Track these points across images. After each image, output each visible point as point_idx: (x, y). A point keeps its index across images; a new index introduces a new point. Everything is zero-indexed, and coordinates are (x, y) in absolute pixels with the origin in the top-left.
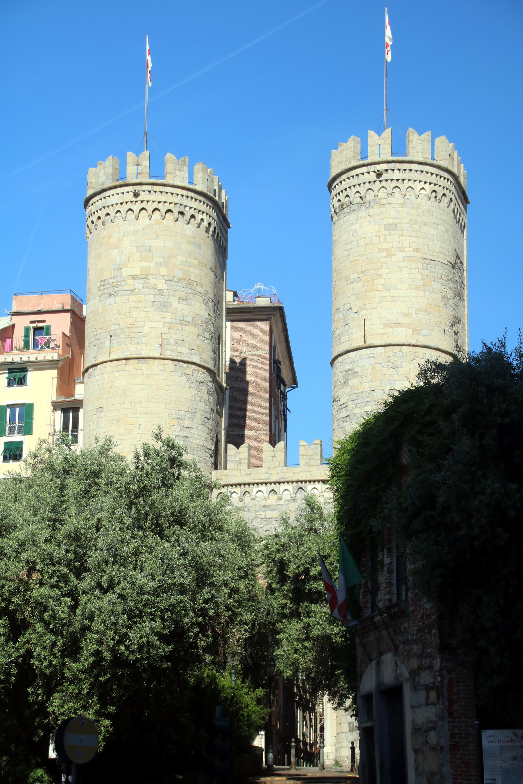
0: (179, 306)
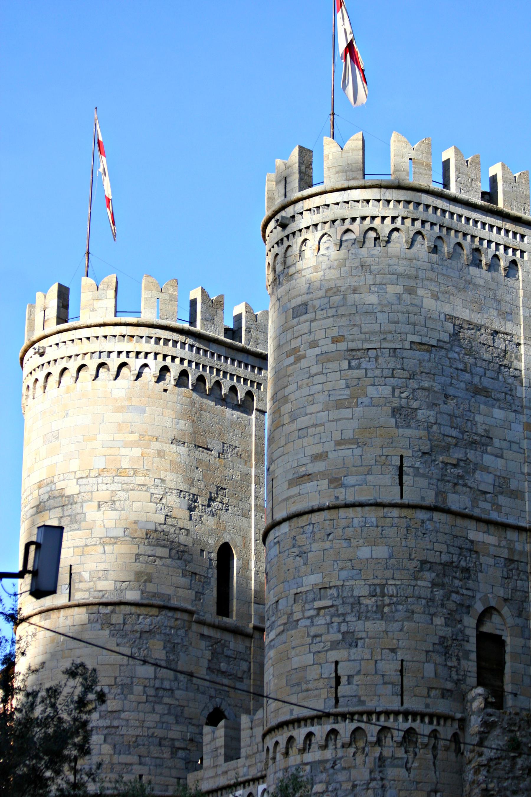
0: (99, 515)
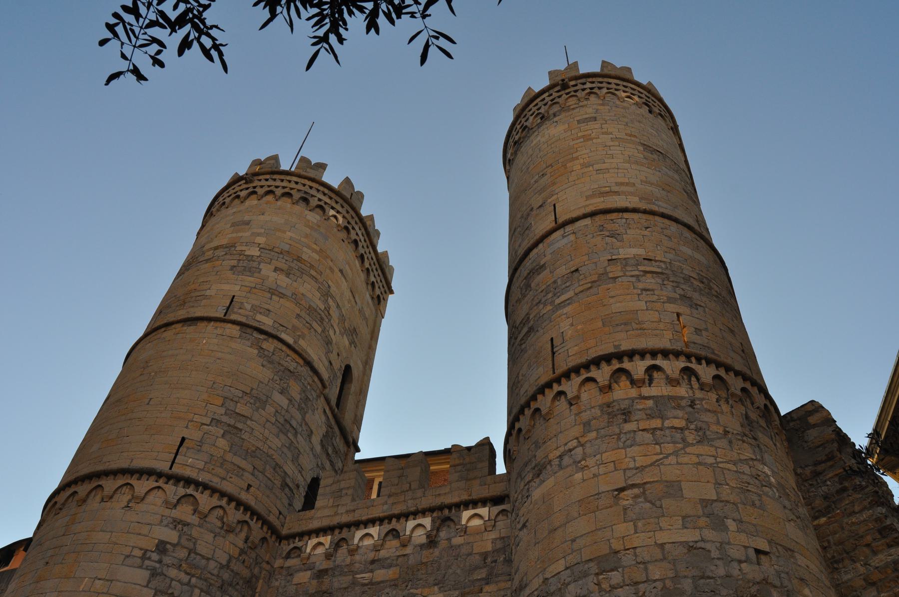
0: (273, 275)
